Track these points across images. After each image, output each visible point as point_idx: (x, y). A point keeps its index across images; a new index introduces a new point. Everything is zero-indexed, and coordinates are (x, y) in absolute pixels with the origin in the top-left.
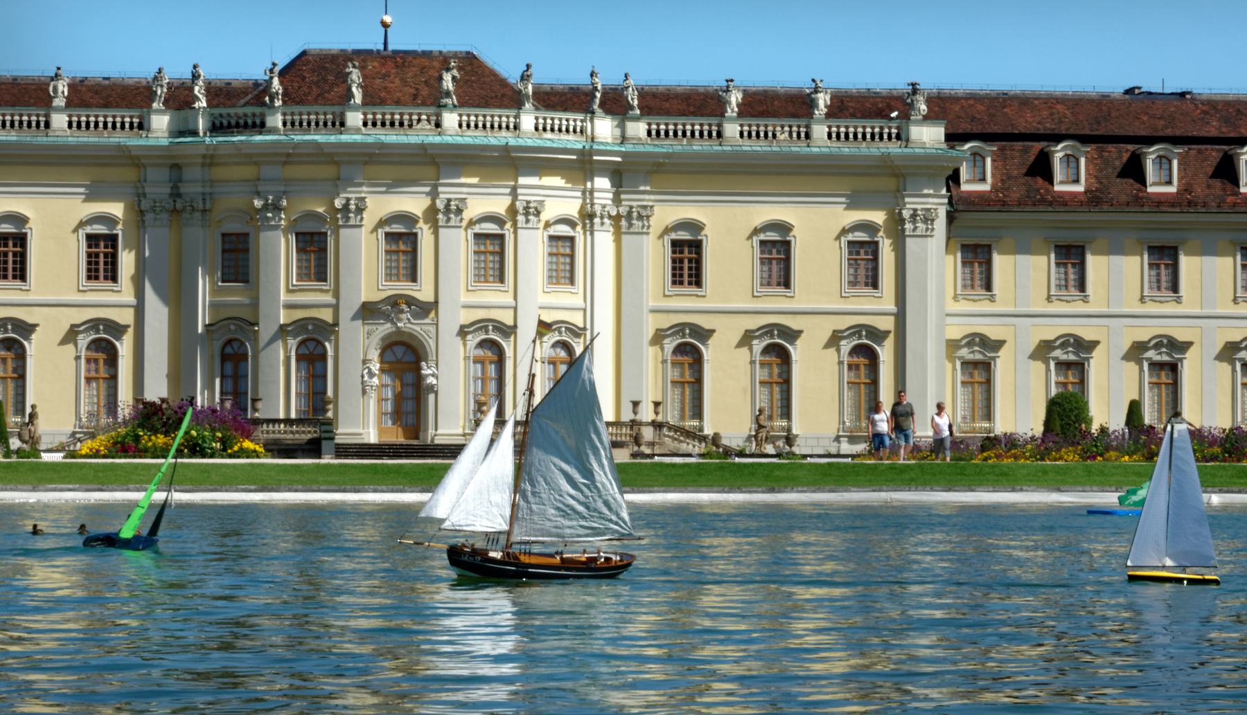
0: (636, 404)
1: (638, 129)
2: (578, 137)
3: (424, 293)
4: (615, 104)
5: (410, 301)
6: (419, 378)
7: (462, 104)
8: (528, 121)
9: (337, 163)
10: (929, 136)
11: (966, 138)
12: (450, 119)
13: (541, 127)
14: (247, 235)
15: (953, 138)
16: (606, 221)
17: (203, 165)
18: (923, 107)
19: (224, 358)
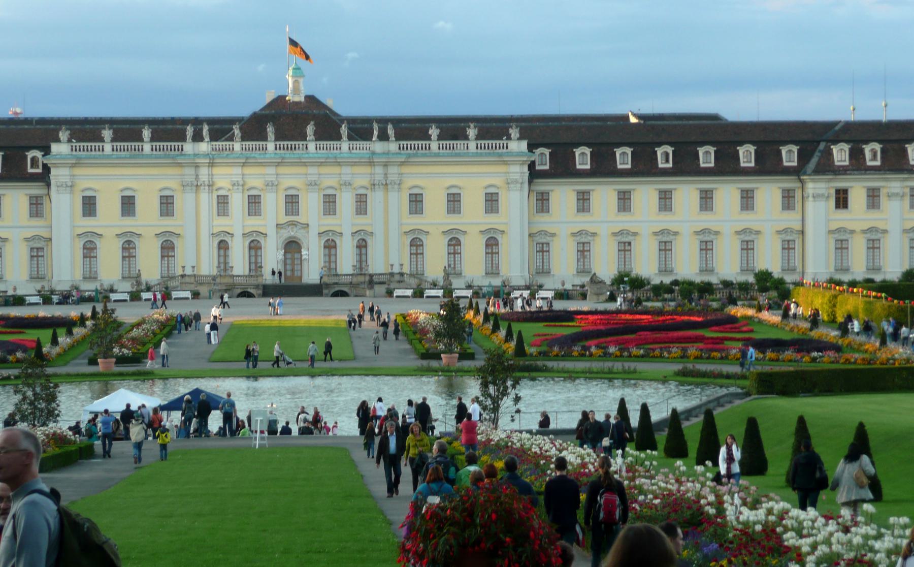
0: (392, 265)
1: (393, 146)
2: (365, 151)
3: (301, 219)
4: (383, 137)
5: (293, 224)
6: (301, 255)
7: (317, 139)
8: (345, 145)
9: (337, 162)
10: (518, 146)
11: (538, 146)
12: (312, 146)
13: (351, 148)
14: (227, 196)
15: (531, 147)
16: (381, 187)
17: (209, 166)
18: (518, 135)
19: (219, 248)
